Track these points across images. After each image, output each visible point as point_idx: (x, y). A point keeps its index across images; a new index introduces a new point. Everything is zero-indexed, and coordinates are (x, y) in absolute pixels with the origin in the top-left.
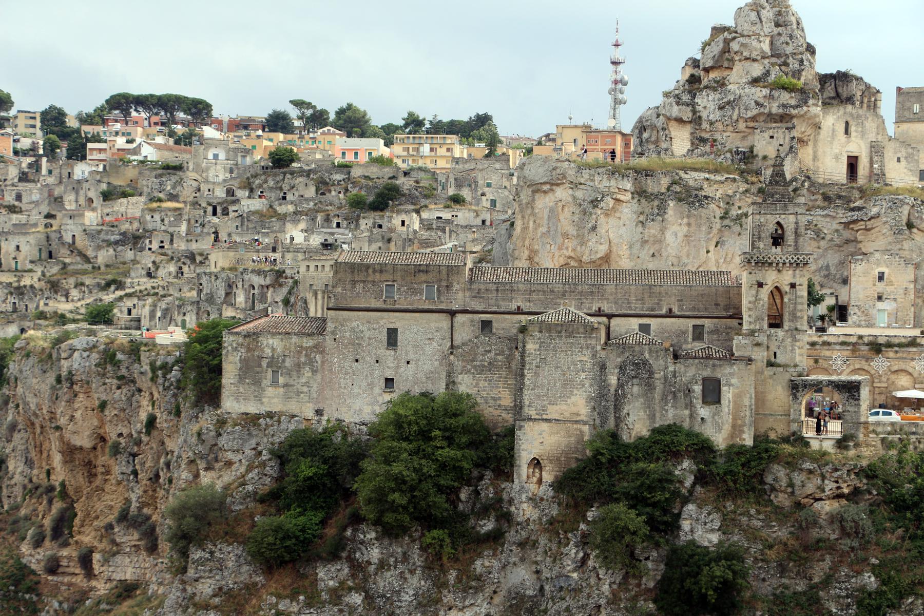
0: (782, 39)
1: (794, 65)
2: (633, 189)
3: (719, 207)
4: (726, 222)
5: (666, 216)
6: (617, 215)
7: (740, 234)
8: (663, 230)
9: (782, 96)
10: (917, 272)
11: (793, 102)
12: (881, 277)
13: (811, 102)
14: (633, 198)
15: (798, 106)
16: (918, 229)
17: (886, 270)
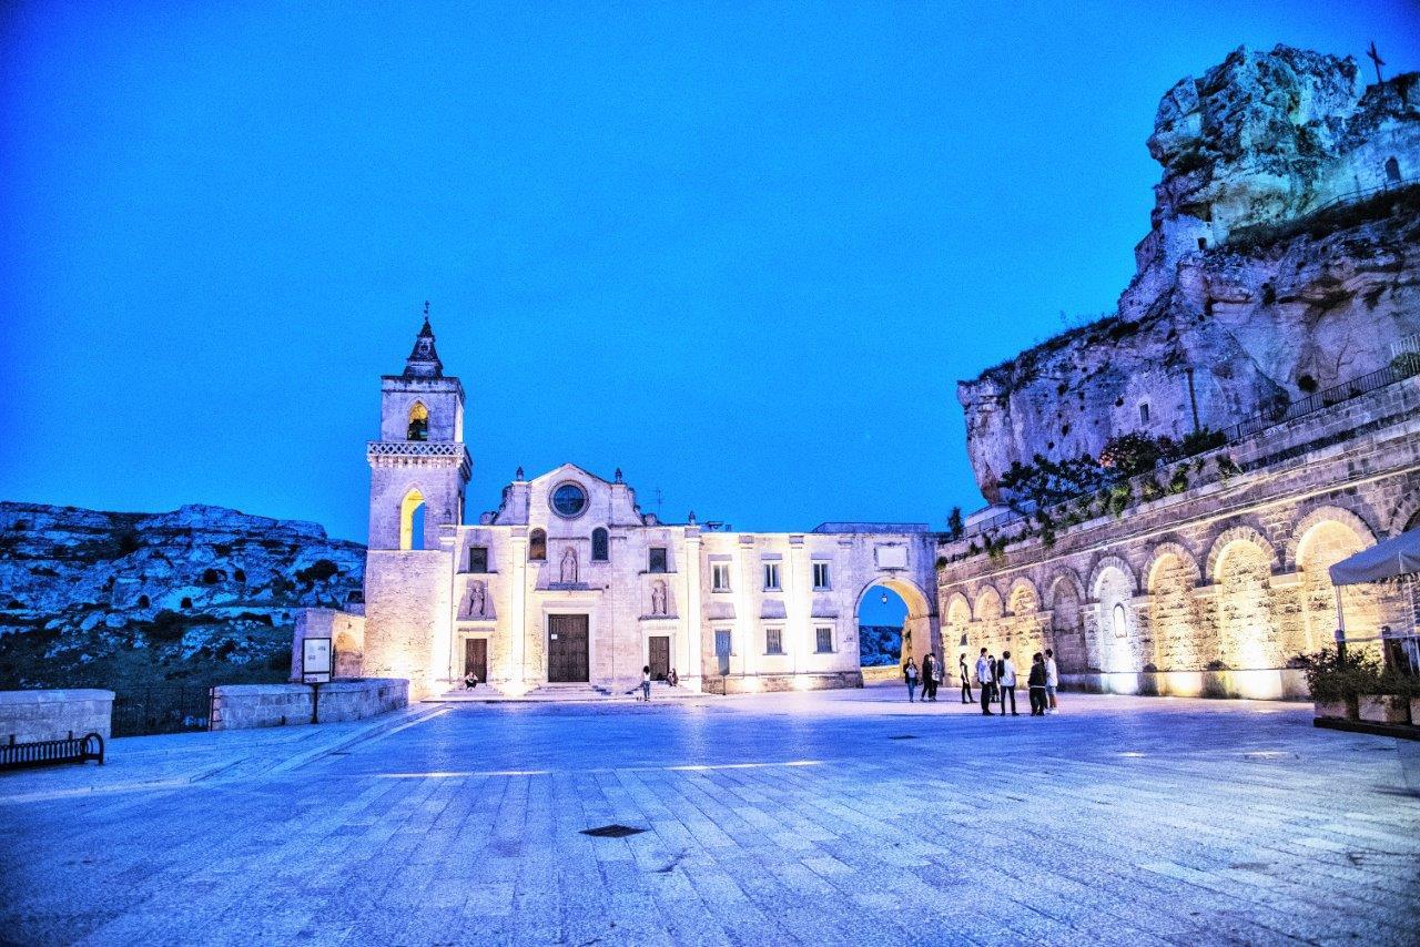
0: (1218, 104)
1: (1229, 129)
2: (997, 392)
3: (1056, 379)
4: (1066, 396)
5: (1011, 413)
6: (992, 429)
7: (1082, 408)
8: (1011, 432)
9: (1178, 186)
10: (1228, 384)
11: (1196, 184)
12: (1145, 408)
13: (1217, 172)
14: (998, 403)
15: (1197, 190)
16: (1226, 301)
17: (1146, 399)
